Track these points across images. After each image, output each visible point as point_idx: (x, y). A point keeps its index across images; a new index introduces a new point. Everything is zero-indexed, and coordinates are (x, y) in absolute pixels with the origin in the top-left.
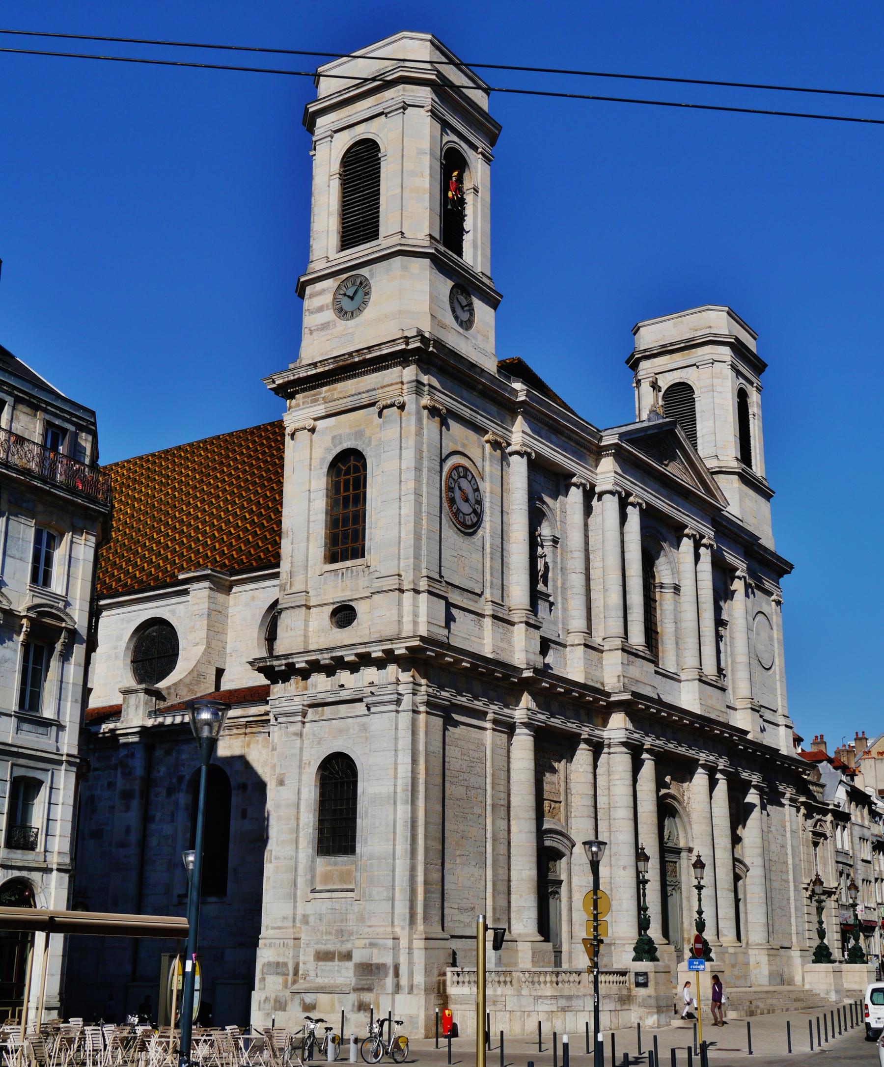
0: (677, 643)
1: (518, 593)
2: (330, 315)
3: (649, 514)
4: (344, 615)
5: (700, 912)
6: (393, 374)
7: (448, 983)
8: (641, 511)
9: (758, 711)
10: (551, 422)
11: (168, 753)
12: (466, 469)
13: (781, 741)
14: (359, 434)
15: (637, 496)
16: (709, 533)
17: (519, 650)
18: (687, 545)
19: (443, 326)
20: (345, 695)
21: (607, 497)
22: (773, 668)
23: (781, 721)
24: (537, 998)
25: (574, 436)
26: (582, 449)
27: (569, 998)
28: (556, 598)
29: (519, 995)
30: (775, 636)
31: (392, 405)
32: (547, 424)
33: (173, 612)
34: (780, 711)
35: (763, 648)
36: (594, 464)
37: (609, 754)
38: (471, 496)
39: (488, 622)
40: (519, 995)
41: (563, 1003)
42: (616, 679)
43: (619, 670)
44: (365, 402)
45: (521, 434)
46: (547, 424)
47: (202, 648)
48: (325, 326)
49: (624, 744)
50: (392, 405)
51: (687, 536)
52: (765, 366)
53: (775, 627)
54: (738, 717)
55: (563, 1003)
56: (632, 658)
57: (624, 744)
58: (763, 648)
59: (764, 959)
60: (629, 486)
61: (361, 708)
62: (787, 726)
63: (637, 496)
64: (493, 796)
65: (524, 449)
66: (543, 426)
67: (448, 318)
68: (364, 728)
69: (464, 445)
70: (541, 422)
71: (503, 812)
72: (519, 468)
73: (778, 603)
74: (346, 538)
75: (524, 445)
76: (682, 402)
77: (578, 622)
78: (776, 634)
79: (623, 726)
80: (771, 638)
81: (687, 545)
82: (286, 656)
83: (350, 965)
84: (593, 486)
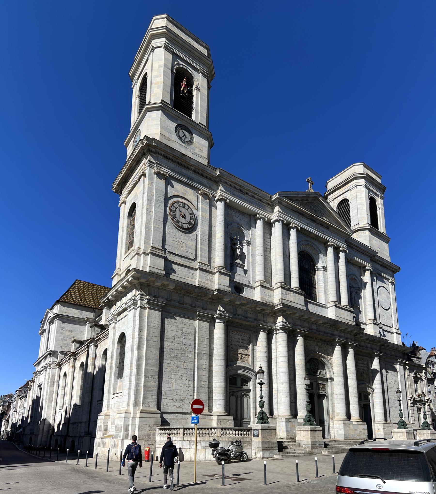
0: (325, 292)
1: (218, 259)
3: (301, 232)
8: (298, 231)
9: (378, 325)
10: (239, 187)
13: (395, 339)
15: (294, 223)
16: (343, 246)
17: (217, 282)
18: (330, 250)
21: (277, 223)
22: (390, 309)
23: (394, 331)
25: (255, 196)
26: (262, 203)
28: (248, 267)
30: (391, 297)
32: (235, 188)
34: (394, 327)
35: (384, 301)
36: (271, 211)
37: (276, 334)
39: (198, 271)
42: (278, 301)
43: (280, 296)
45: (220, 191)
46: (237, 189)
49: (281, 329)
51: (331, 246)
53: (391, 293)
54: (368, 328)
56: (288, 292)
57: (281, 329)
58: (384, 301)
59: (381, 428)
60: (289, 219)
62: (397, 333)
63: (294, 223)
64: (198, 349)
65: (221, 197)
66: (235, 189)
70: (234, 187)
71: (206, 357)
72: (220, 206)
73: (392, 283)
75: (221, 195)
76: (345, 207)
77: (259, 276)
78: (392, 296)
79: (281, 320)
80: (389, 298)
81: (330, 250)
84: (269, 220)
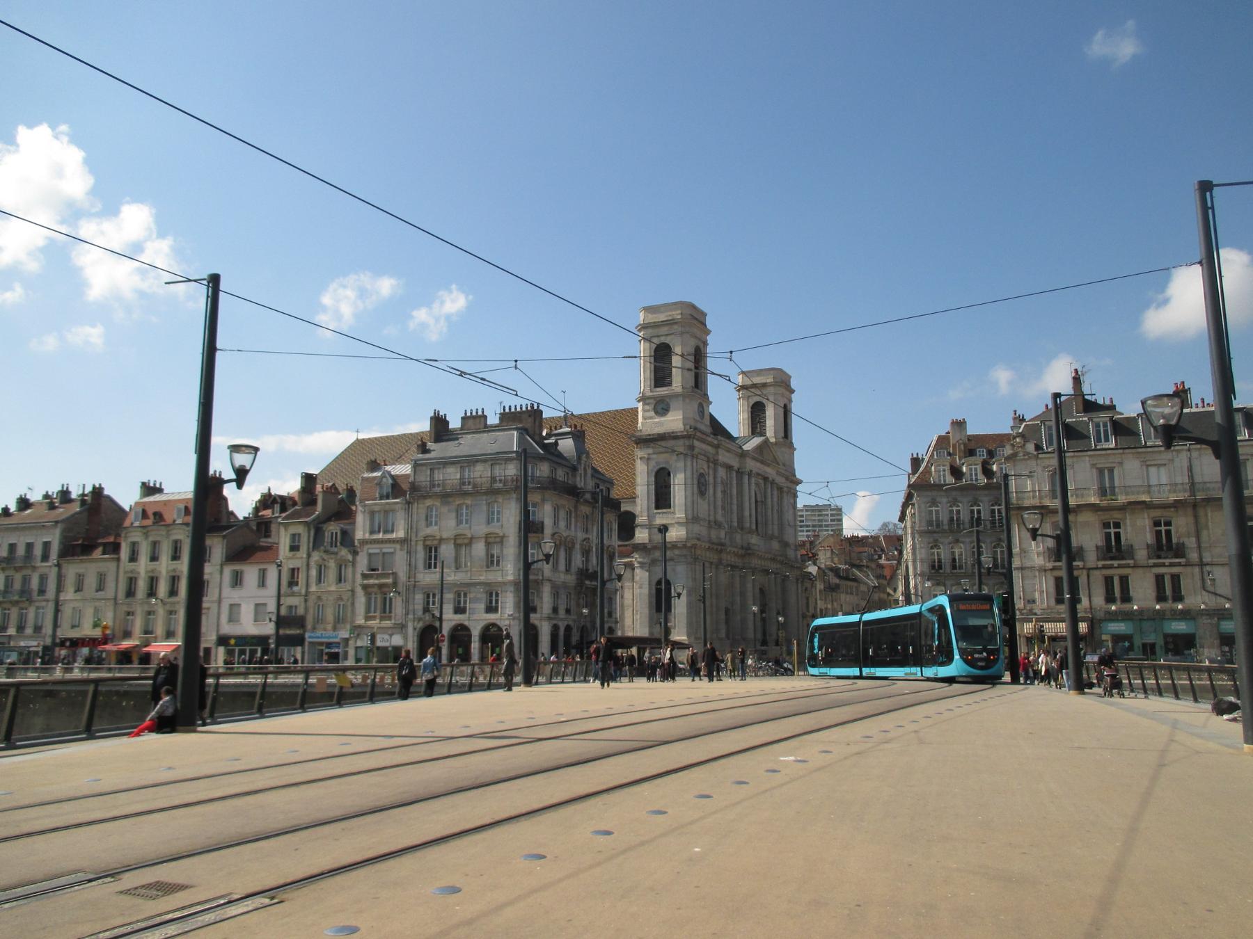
2: (652, 413)
6: (681, 442)
14: (667, 462)
74: (662, 499)
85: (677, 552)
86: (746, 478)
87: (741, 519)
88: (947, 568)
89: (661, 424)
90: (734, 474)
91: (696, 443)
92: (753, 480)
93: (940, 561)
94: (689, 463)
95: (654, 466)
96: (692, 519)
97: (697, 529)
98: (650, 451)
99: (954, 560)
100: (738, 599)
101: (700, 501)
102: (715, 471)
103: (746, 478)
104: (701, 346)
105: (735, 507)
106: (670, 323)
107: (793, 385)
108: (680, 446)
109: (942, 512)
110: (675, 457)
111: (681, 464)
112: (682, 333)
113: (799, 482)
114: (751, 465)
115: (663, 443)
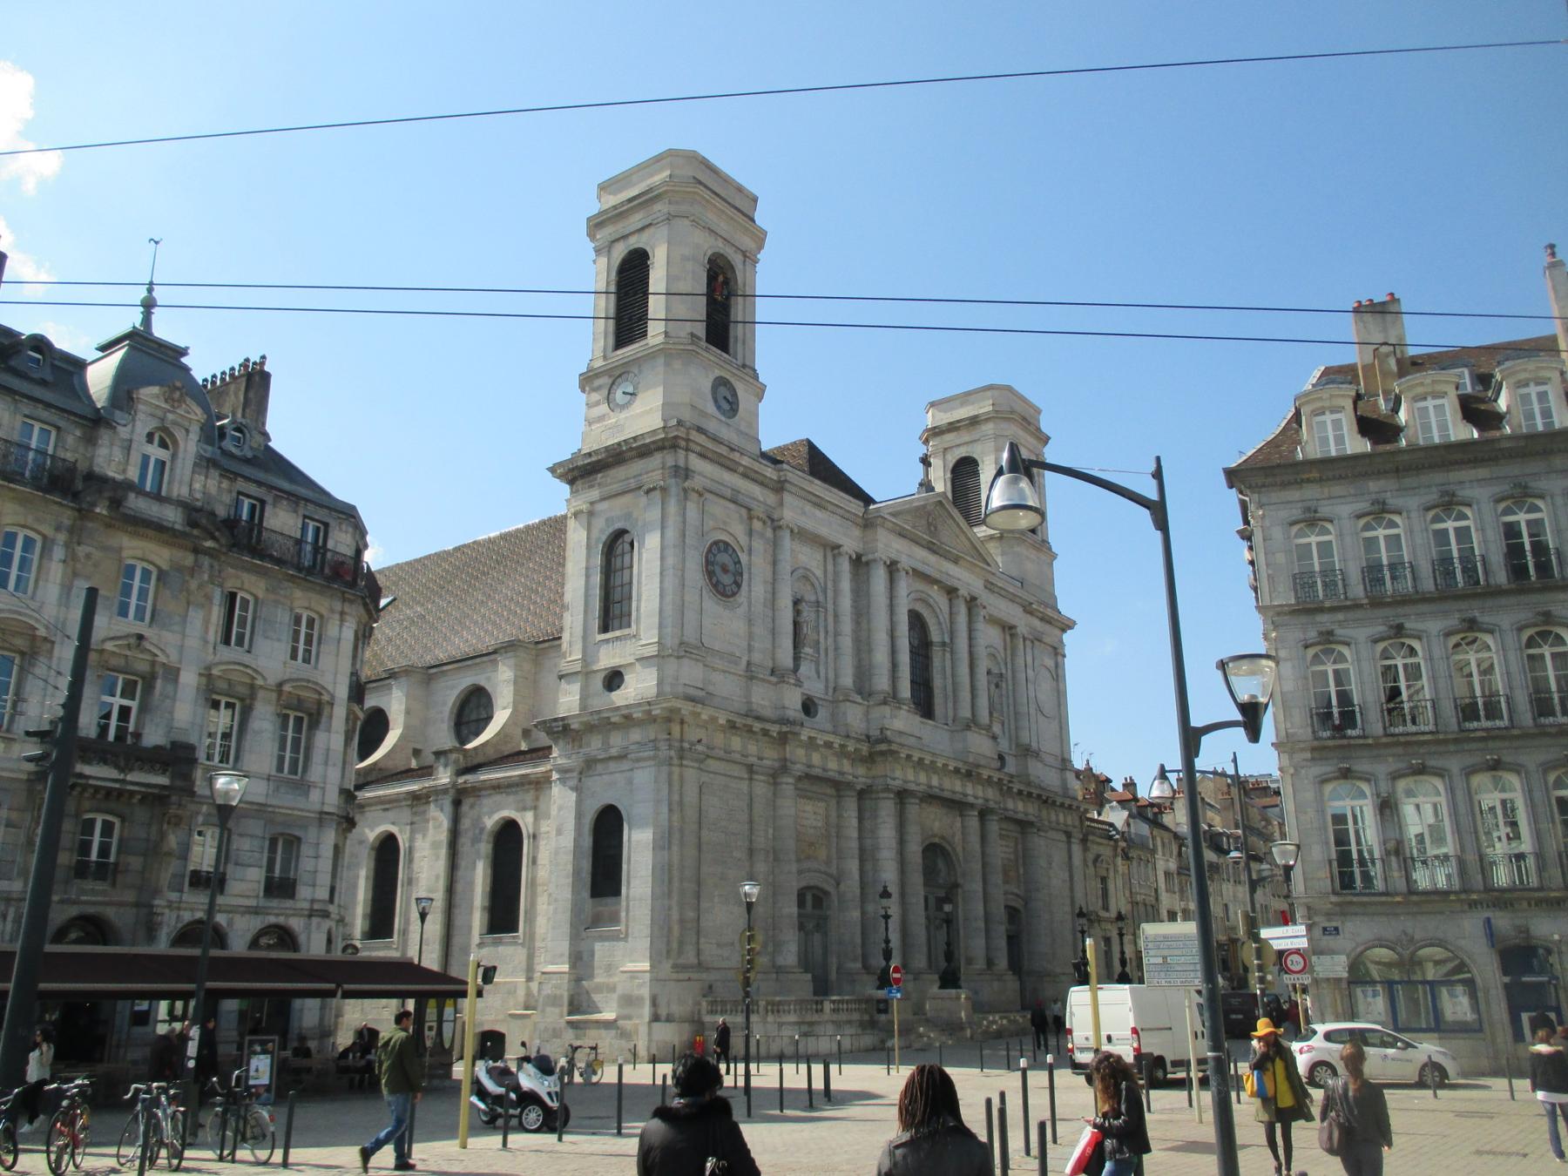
2: (604, 408)
4: (614, 679)
5: (887, 941)
6: (656, 460)
7: (704, 1012)
11: (472, 807)
12: (727, 544)
14: (628, 516)
19: (703, 414)
20: (614, 752)
24: (780, 1025)
27: (811, 1024)
29: (765, 1022)
31: (654, 489)
33: (488, 679)
38: (731, 567)
40: (765, 1022)
41: (805, 1028)
44: (633, 486)
47: (508, 712)
48: (601, 418)
50: (654, 489)
52: (1048, 438)
55: (805, 1028)
61: (625, 765)
67: (711, 408)
68: (630, 782)
69: (725, 523)
82: (563, 719)
83: (615, 996)
85: (636, 735)
86: (879, 578)
87: (863, 673)
88: (1373, 722)
89: (618, 427)
90: (845, 566)
91: (696, 463)
92: (904, 586)
93: (1344, 698)
94: (672, 508)
95: (602, 531)
96: (680, 648)
97: (691, 673)
98: (595, 494)
99: (1394, 693)
100: (853, 866)
101: (711, 605)
102: (775, 544)
103: (879, 578)
104: (737, 260)
105: (847, 643)
106: (645, 200)
107: (1046, 425)
108: (652, 469)
109: (1343, 540)
110: (644, 500)
111: (654, 514)
112: (670, 218)
113: (1067, 625)
114: (887, 545)
115: (620, 473)
